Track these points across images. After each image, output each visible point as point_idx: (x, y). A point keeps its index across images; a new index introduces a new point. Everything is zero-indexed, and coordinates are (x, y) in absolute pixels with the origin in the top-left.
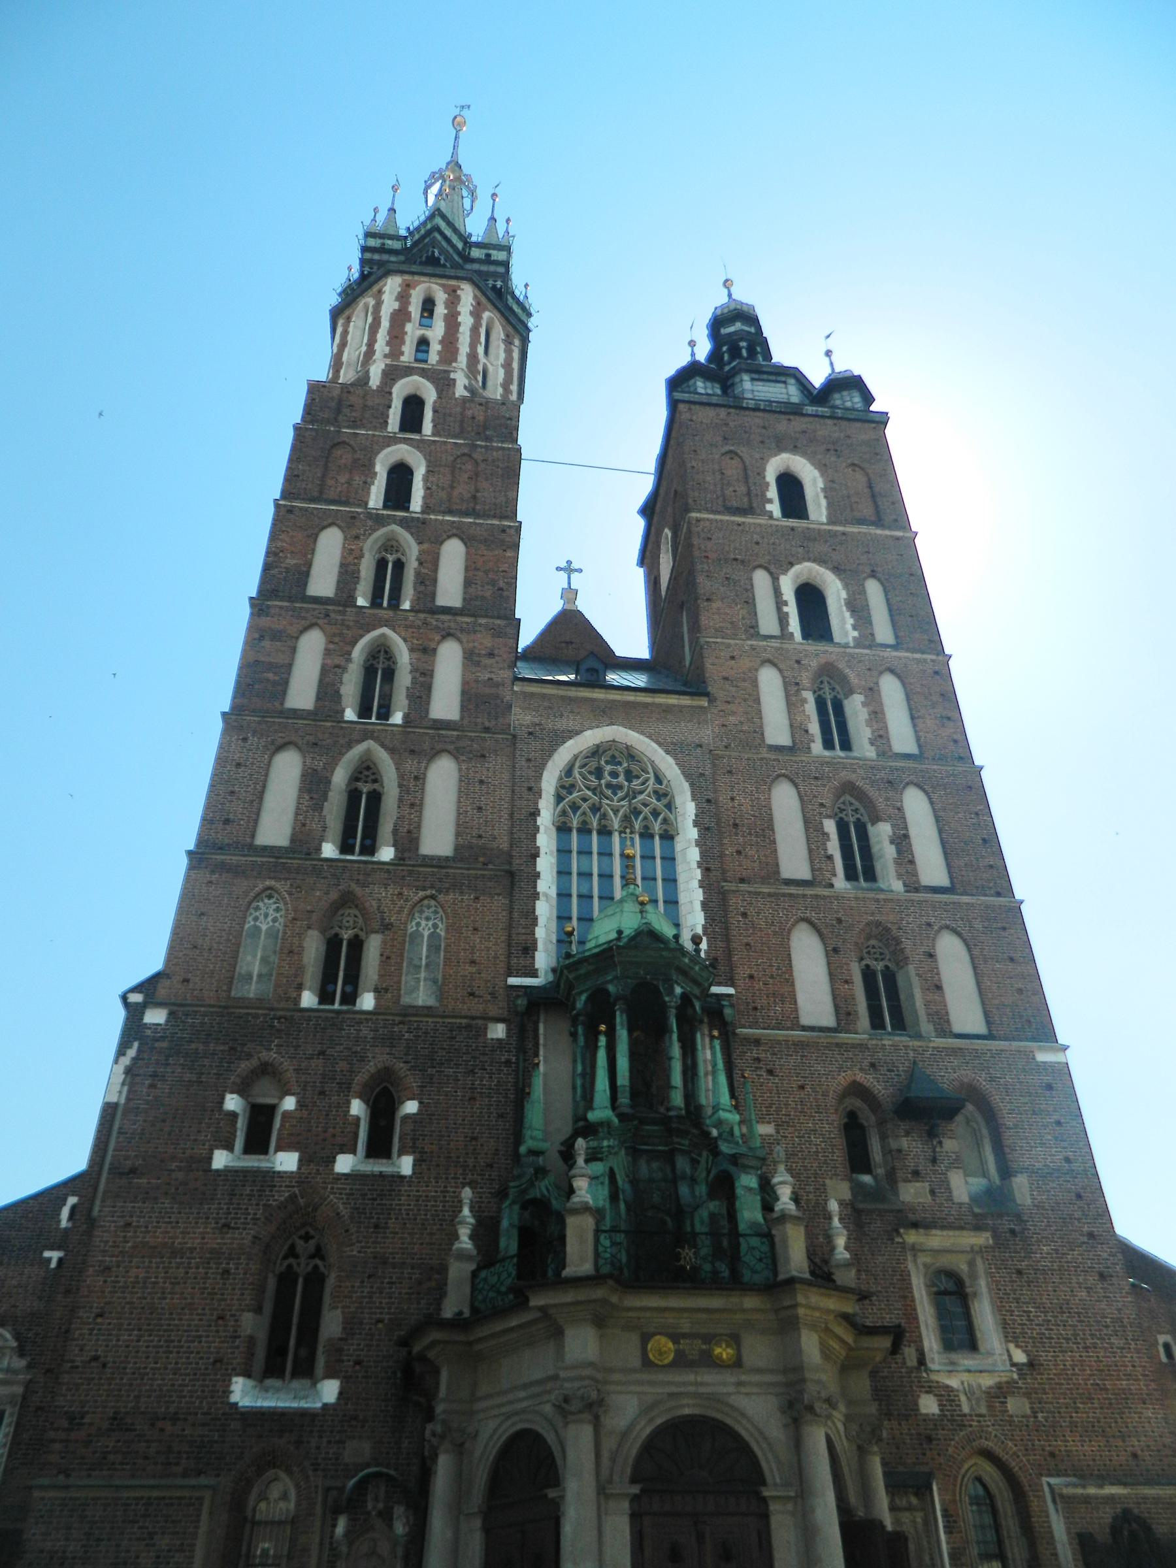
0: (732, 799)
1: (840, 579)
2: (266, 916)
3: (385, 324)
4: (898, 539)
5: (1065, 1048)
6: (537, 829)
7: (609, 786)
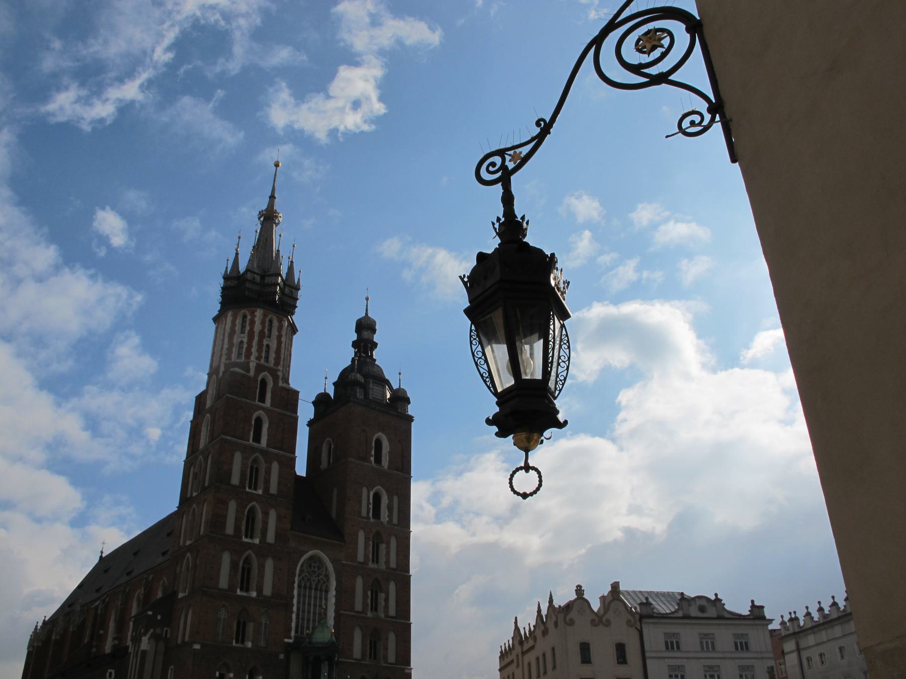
2: (223, 613)
3: (256, 338)
5: (411, 669)
6: (294, 588)
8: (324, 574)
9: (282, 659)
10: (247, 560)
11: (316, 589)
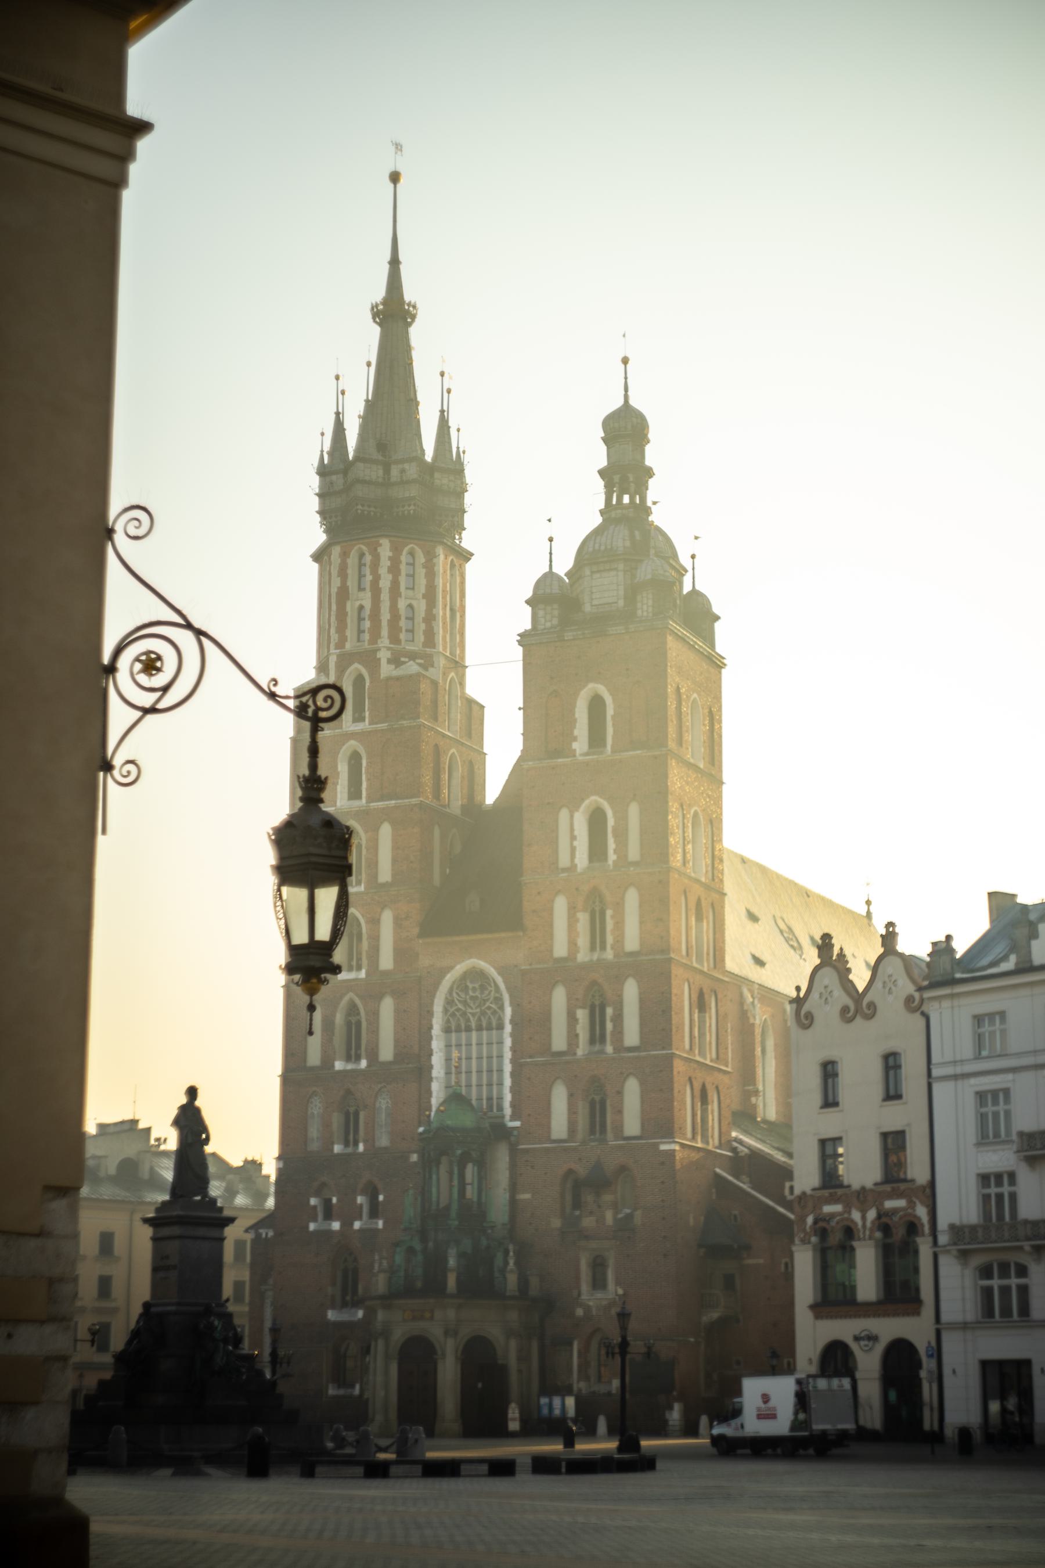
0: (530, 1003)
1: (612, 808)
2: (316, 1106)
3: (334, 607)
4: (655, 757)
6: (431, 1038)
7: (472, 998)
8: (492, 999)
9: (415, 1162)
10: (353, 1009)
11: (479, 1028)
